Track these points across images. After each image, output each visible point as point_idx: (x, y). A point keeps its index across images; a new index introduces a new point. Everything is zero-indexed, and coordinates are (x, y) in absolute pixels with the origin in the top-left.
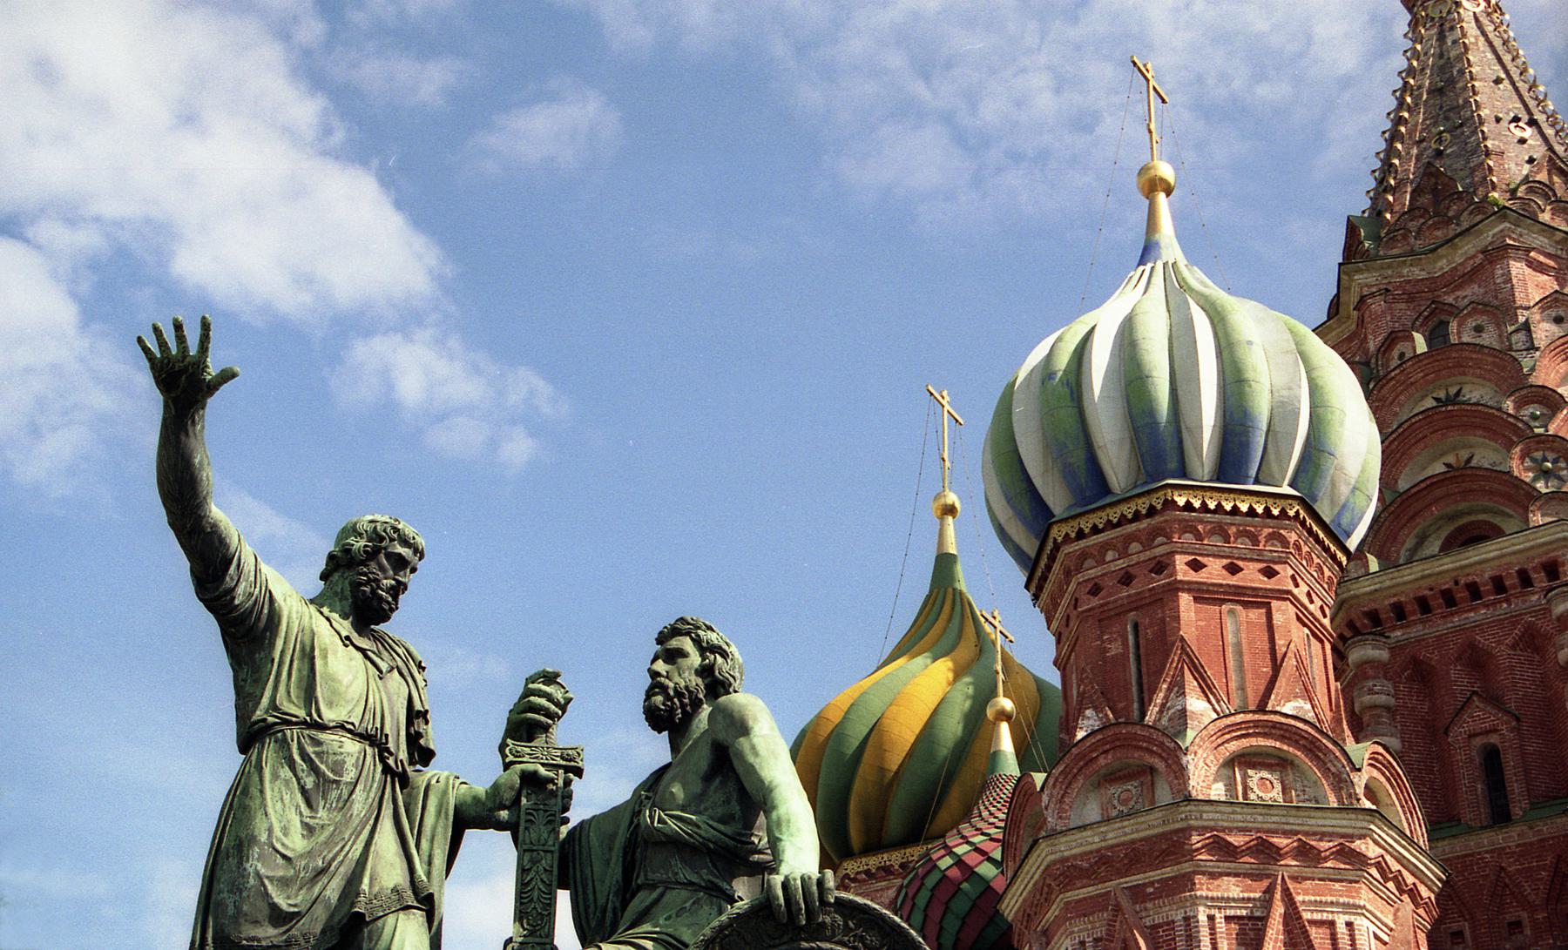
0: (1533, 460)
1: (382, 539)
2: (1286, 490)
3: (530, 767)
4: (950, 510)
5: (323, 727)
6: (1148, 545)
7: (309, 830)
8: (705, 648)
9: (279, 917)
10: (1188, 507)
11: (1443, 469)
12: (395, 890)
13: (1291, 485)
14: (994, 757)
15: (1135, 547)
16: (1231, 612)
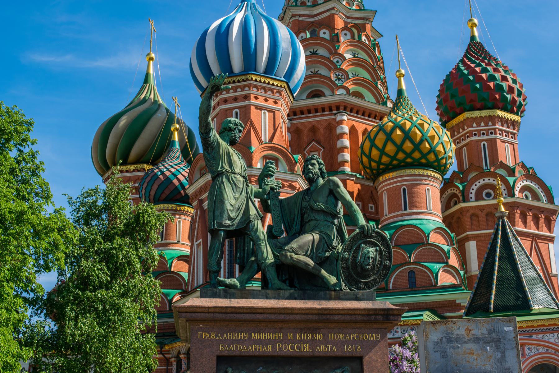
0: (336, 75)
1: (237, 125)
2: (283, 79)
3: (272, 186)
4: (152, 59)
5: (235, 174)
6: (243, 90)
7: (235, 198)
8: (319, 164)
9: (230, 218)
10: (256, 80)
11: (311, 73)
12: (255, 214)
13: (284, 77)
14: (174, 141)
15: (239, 90)
16: (265, 113)
